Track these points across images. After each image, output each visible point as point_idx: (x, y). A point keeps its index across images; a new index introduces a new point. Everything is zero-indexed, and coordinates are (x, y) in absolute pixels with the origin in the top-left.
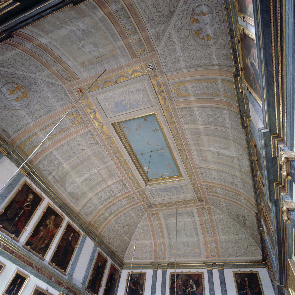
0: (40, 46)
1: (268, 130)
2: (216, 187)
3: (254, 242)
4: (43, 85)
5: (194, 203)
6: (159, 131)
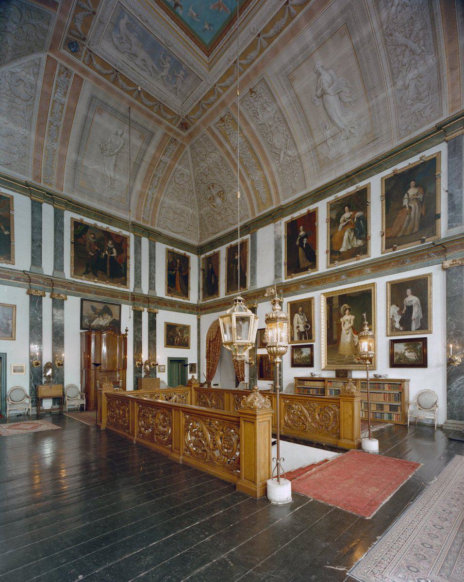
5: (170, 121)
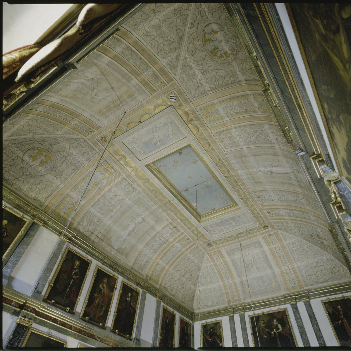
0: (53, 106)
1: (305, 153)
2: (279, 209)
3: (339, 262)
4: (64, 143)
5: (258, 231)
6: (200, 163)
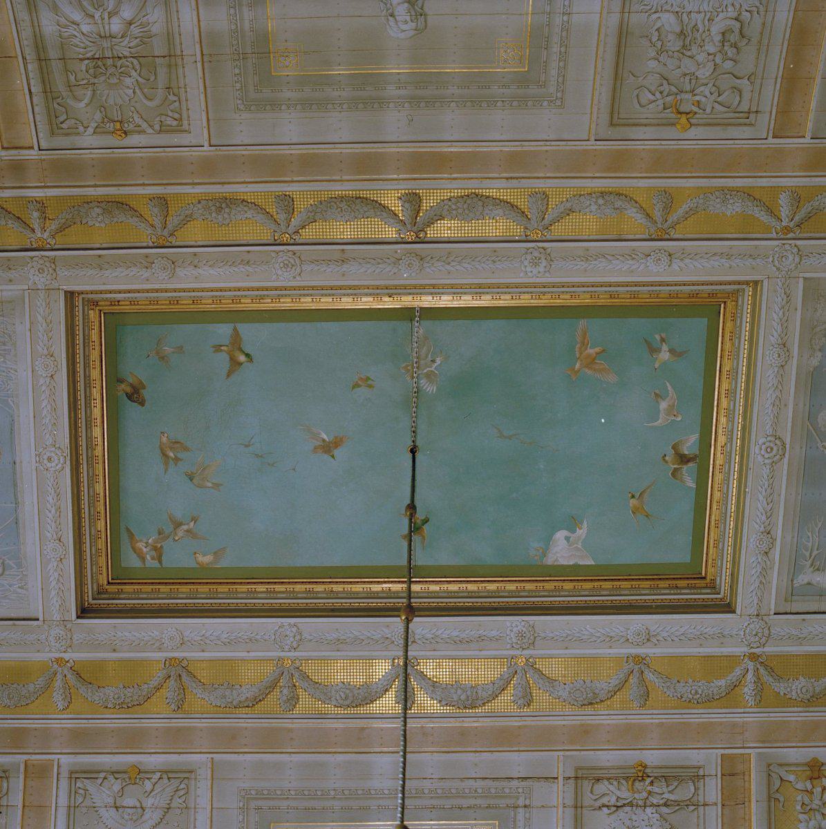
6: (252, 334)
